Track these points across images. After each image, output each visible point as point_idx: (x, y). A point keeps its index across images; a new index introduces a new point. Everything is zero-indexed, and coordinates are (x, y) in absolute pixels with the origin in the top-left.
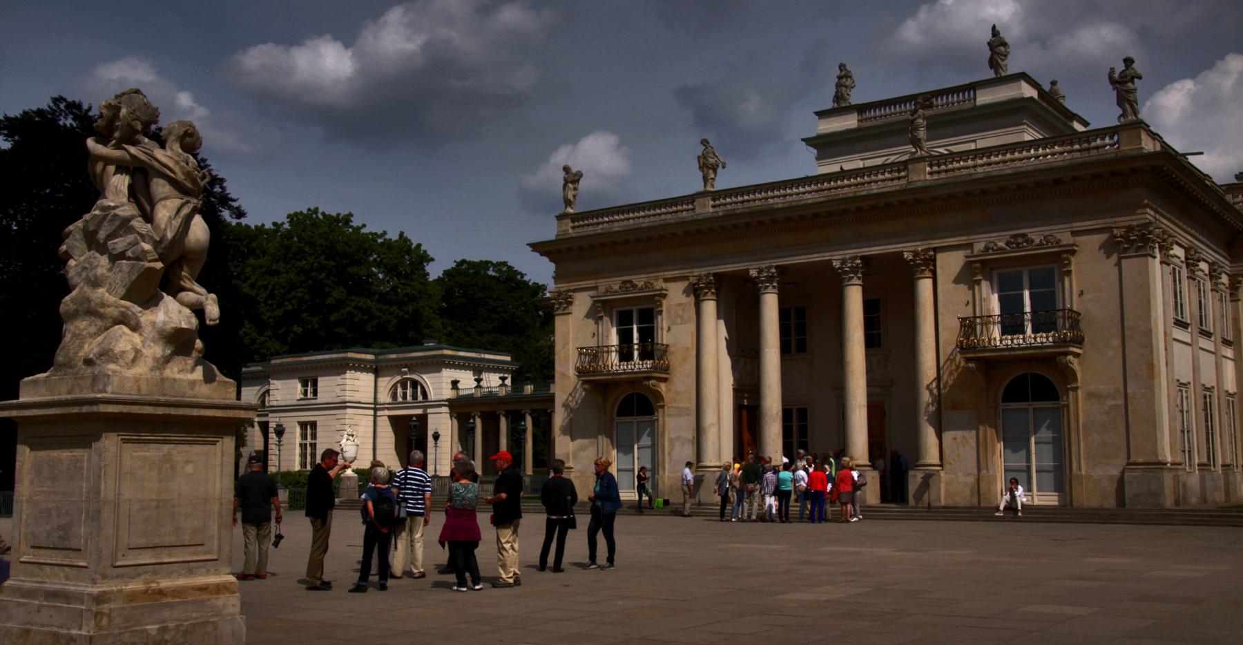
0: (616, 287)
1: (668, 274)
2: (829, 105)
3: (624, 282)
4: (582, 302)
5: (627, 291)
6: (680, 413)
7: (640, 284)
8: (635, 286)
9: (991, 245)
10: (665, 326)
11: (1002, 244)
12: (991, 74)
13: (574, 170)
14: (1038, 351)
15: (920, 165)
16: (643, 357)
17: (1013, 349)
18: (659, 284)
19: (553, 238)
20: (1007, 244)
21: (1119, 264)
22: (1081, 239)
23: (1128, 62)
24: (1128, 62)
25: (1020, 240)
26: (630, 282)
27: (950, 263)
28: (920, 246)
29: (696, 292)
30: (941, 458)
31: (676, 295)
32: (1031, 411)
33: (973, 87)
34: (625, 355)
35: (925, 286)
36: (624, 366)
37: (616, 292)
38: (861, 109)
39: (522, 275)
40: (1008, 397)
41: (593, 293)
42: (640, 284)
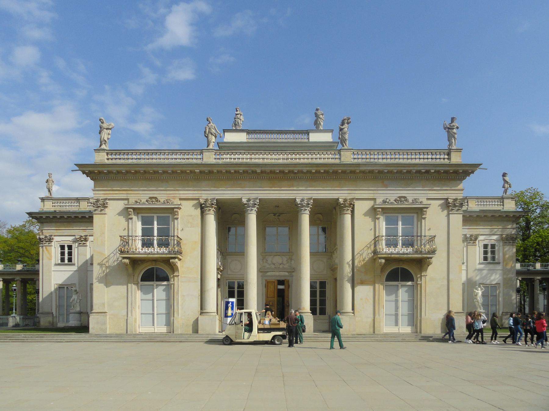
0: (144, 200)
3: (151, 198)
4: (115, 207)
7: (162, 201)
11: (392, 201)
16: (160, 245)
21: (448, 215)
25: (403, 199)
26: (156, 198)
27: (362, 207)
29: (203, 208)
34: (147, 244)
41: (126, 202)
42: (162, 201)
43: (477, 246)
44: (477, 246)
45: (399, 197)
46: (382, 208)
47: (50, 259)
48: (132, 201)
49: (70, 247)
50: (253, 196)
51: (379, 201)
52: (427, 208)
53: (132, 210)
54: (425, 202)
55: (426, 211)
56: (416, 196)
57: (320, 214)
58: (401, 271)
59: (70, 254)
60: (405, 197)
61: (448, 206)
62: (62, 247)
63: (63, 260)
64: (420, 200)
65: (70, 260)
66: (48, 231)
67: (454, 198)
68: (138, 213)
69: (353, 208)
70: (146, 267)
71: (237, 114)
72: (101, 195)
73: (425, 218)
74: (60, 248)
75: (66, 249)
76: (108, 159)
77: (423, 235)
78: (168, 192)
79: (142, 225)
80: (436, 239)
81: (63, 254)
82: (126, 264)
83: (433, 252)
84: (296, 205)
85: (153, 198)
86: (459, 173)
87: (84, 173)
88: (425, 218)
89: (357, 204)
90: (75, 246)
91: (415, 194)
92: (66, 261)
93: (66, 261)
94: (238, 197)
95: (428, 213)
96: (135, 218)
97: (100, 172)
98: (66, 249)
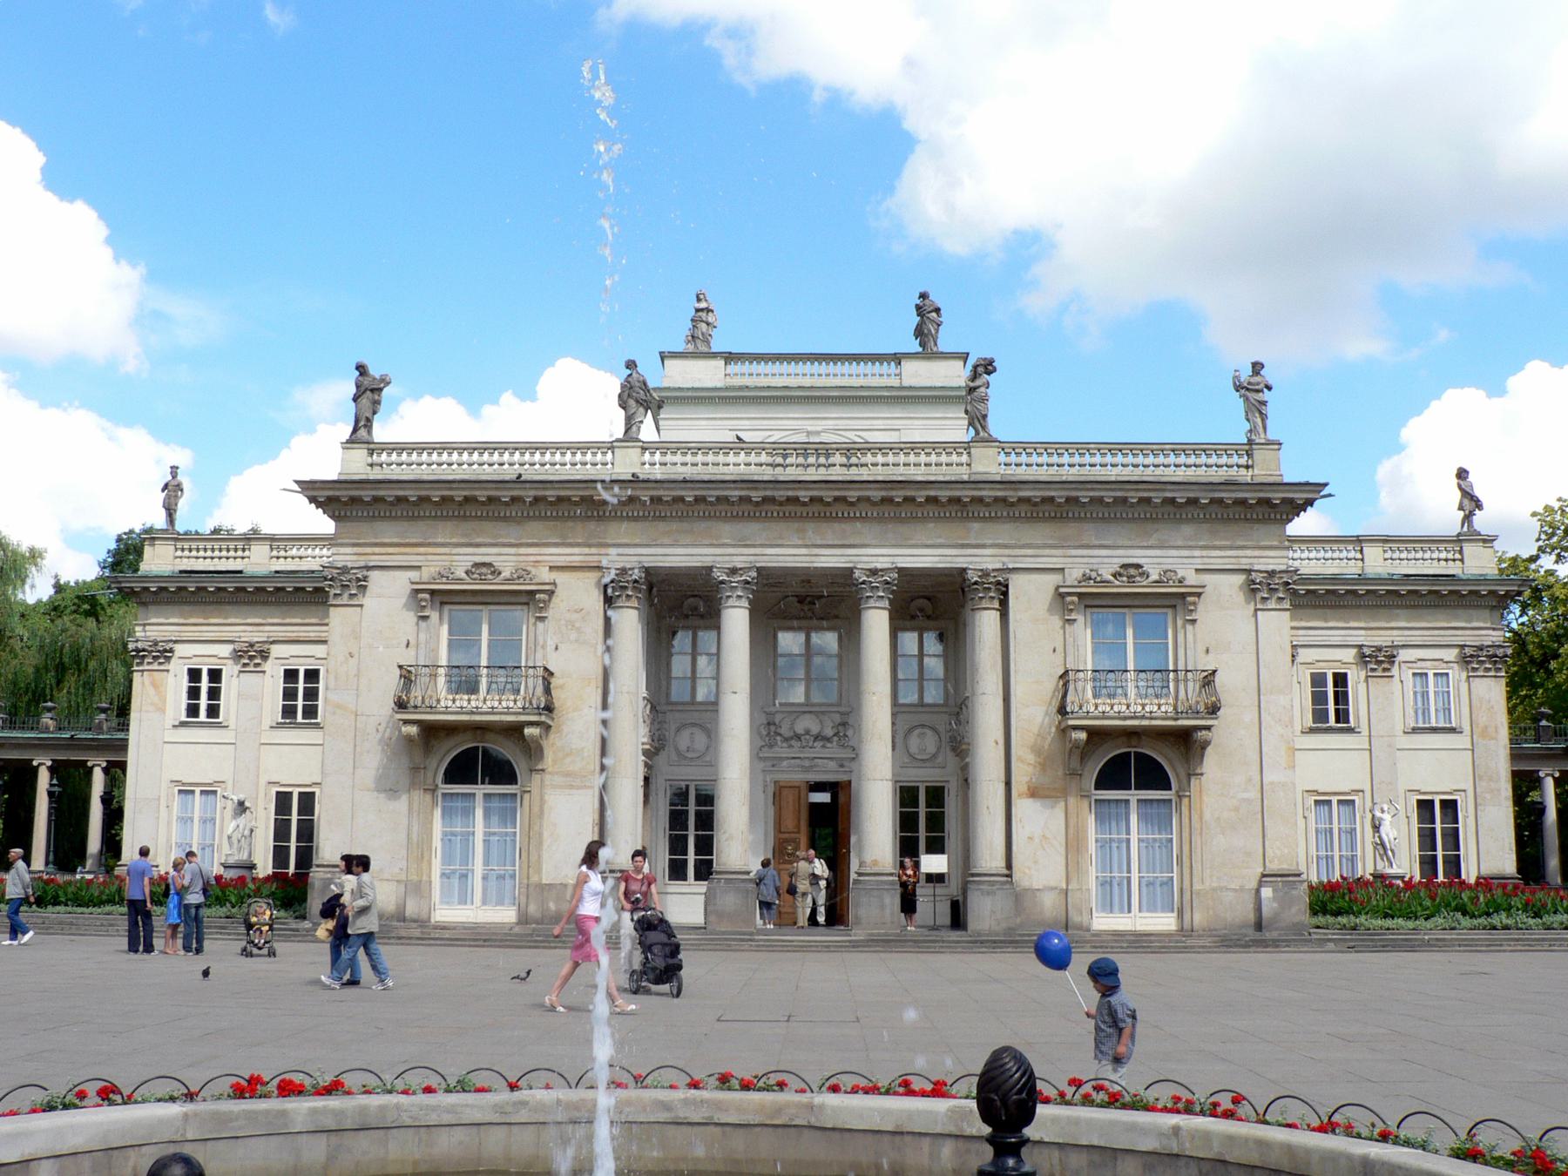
1: (561, 561)
2: (680, 347)
3: (476, 565)
5: (483, 580)
6: (573, 781)
7: (506, 574)
8: (496, 573)
9: (1094, 575)
10: (551, 644)
12: (914, 346)
13: (375, 371)
14: (1145, 723)
15: (992, 452)
17: (1143, 717)
18: (545, 575)
19: (335, 478)
20: (1114, 576)
22: (1207, 579)
23: (1257, 367)
24: (1257, 367)
26: (489, 565)
27: (1031, 595)
28: (990, 564)
30: (1009, 866)
31: (578, 596)
32: (1133, 805)
33: (897, 358)
35: (986, 623)
36: (463, 701)
37: (459, 580)
38: (730, 358)
39: (131, 532)
40: (1101, 784)
41: (414, 575)
43: (1397, 678)
44: (1397, 678)
45: (1124, 566)
46: (1080, 595)
47: (162, 710)
48: (426, 574)
49: (215, 675)
50: (739, 562)
51: (1074, 575)
52: (1199, 595)
53: (427, 596)
54: (1192, 579)
55: (1194, 604)
56: (1169, 563)
57: (929, 599)
58: (1137, 763)
59: (214, 694)
60: (1138, 566)
61: (1260, 588)
62: (194, 675)
63: (193, 711)
64: (1181, 574)
65: (213, 711)
66: (152, 628)
67: (1270, 568)
68: (442, 603)
69: (1006, 594)
70: (456, 746)
71: (698, 310)
72: (345, 557)
73: (1194, 621)
74: (186, 678)
75: (205, 677)
76: (371, 465)
77: (1181, 666)
78: (522, 550)
79: (450, 633)
80: (1218, 679)
81: (194, 693)
82: (409, 739)
83: (1214, 710)
84: (856, 584)
85: (484, 564)
86: (1287, 502)
87: (312, 500)
88: (1194, 621)
89: (1017, 585)
90: (229, 671)
91: (1166, 558)
92: (203, 716)
93: (203, 716)
94: (707, 561)
95: (1200, 607)
96: (434, 616)
97: (354, 500)
98: (205, 677)
